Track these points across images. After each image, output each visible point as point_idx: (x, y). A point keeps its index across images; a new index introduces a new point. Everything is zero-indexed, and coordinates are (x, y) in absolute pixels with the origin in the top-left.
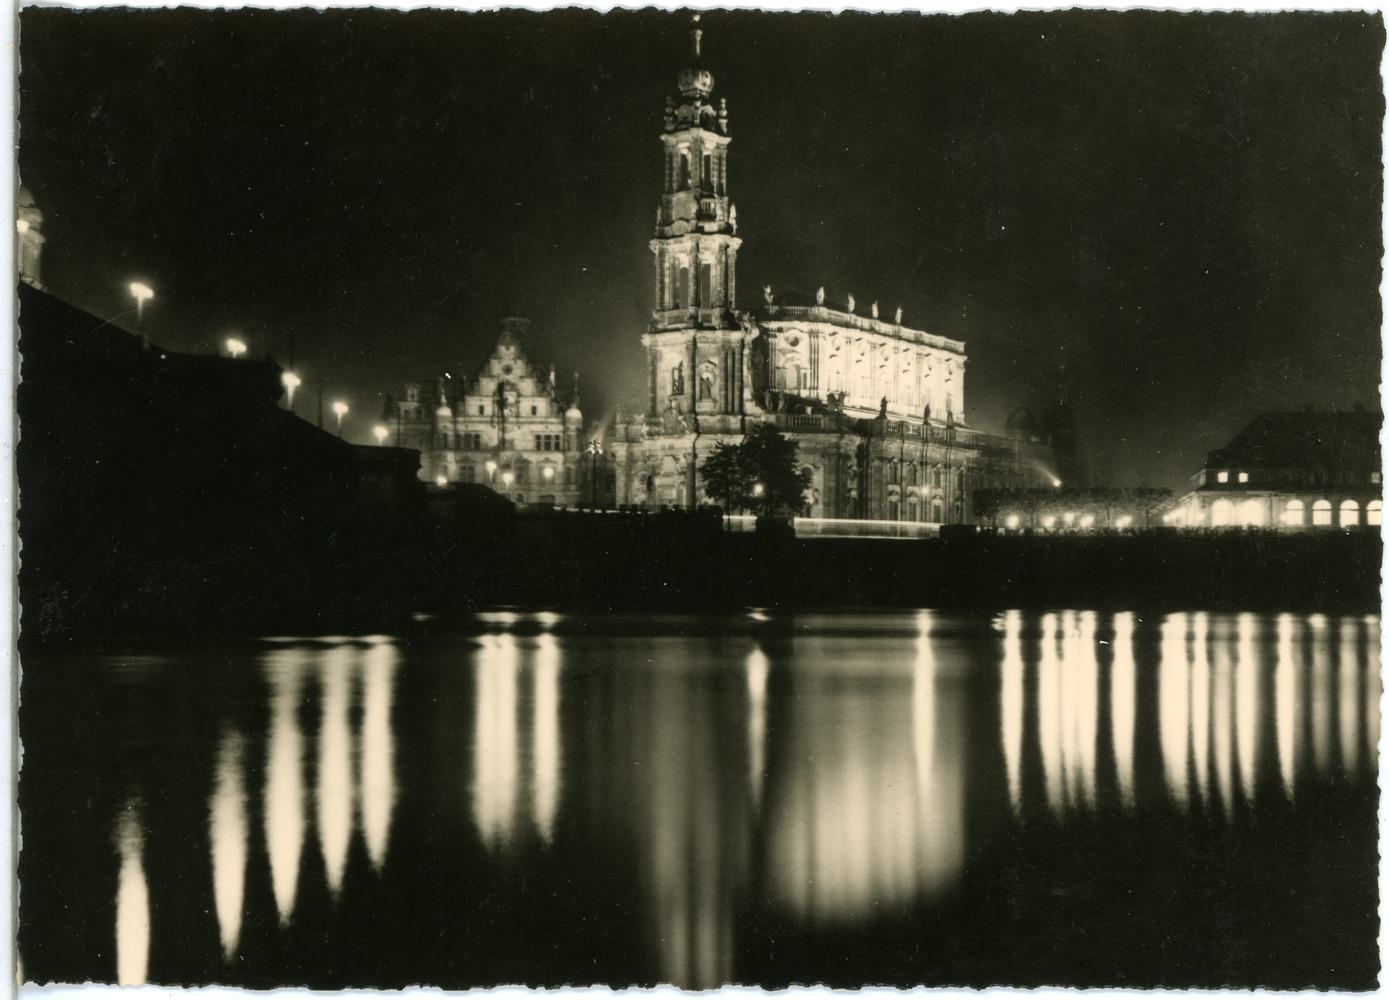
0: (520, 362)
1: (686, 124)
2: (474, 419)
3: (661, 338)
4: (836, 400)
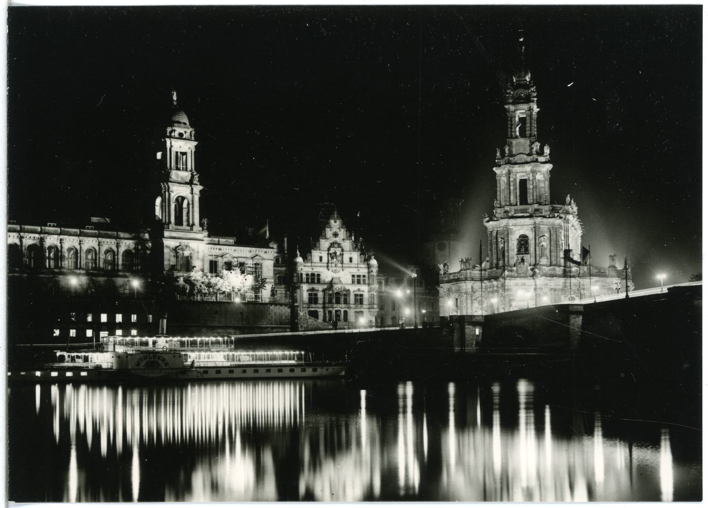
0: (342, 230)
2: (316, 264)
3: (512, 221)
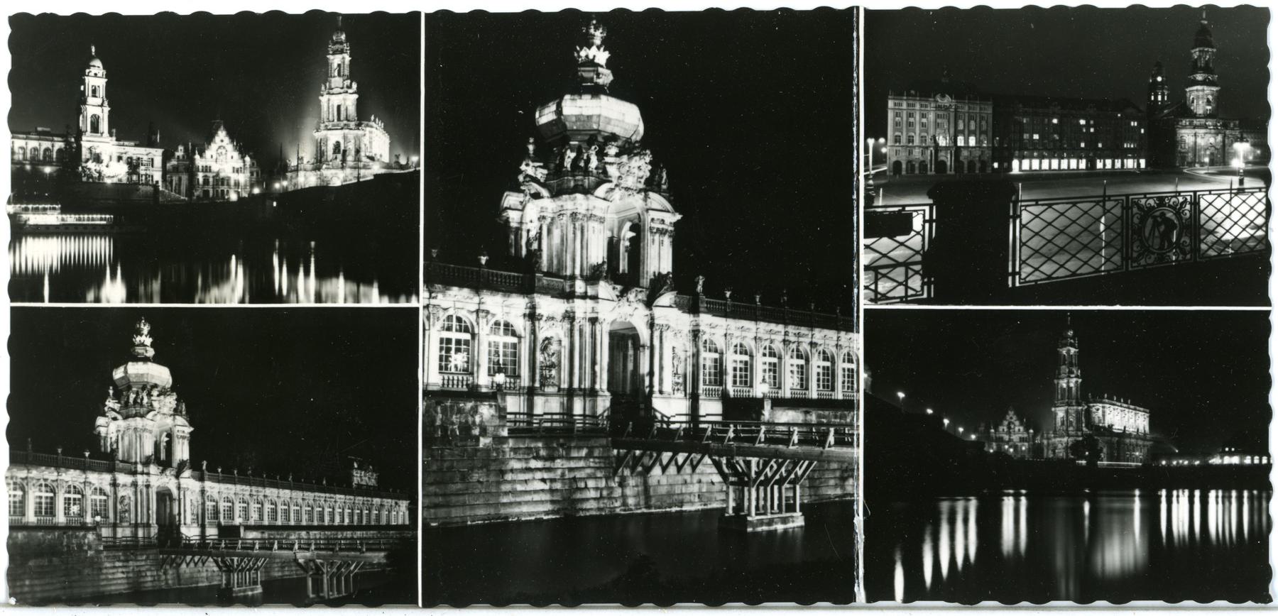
1: (1065, 345)
4: (1111, 426)
